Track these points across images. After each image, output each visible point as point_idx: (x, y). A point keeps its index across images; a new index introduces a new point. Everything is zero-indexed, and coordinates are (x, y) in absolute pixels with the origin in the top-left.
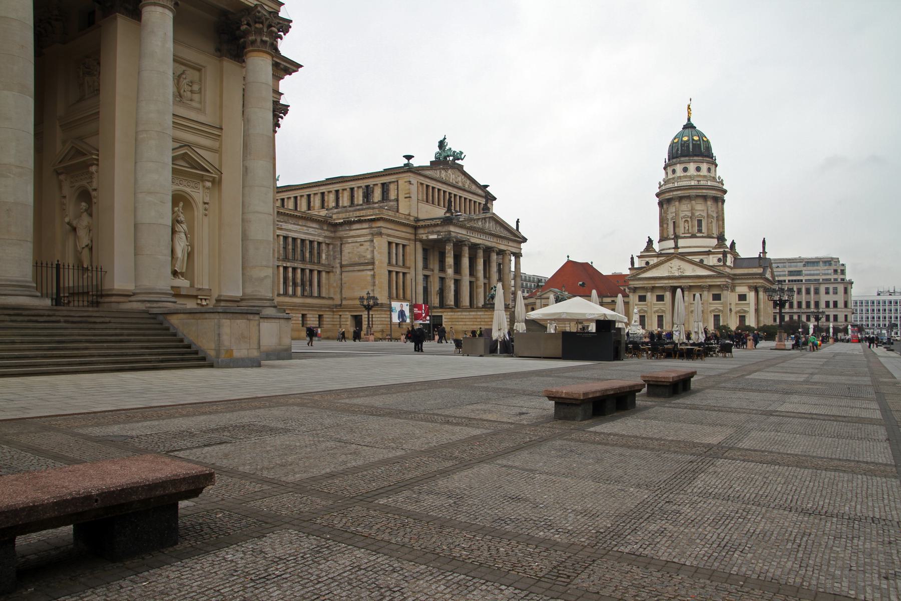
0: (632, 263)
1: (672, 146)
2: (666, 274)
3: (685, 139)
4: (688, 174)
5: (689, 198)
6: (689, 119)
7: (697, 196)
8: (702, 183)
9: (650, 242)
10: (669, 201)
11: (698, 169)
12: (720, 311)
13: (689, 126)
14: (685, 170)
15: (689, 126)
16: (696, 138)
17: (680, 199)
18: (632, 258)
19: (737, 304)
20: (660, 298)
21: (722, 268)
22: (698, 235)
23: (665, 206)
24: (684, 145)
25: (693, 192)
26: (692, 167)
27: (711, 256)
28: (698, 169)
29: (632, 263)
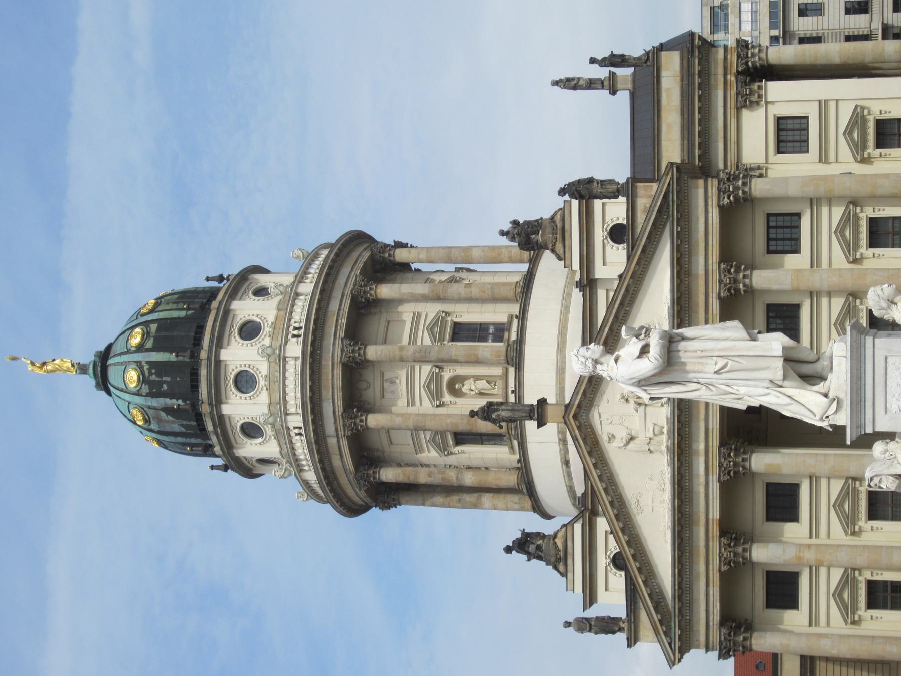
0: (607, 626)
1: (166, 439)
2: (661, 467)
3: (132, 375)
4: (262, 369)
5: (355, 370)
6: (82, 369)
7: (355, 333)
8: (299, 315)
9: (525, 544)
10: (367, 456)
11: (250, 331)
12: (850, 220)
13: (101, 369)
14: (245, 382)
15: (101, 369)
16: (136, 339)
17: (356, 402)
18: (583, 625)
19: (823, 158)
20: (783, 502)
21: (642, 203)
22: (513, 337)
23: (389, 475)
24: (154, 381)
25: (334, 350)
26: (238, 355)
27: (600, 272)
28: (250, 331)
29: (607, 626)
